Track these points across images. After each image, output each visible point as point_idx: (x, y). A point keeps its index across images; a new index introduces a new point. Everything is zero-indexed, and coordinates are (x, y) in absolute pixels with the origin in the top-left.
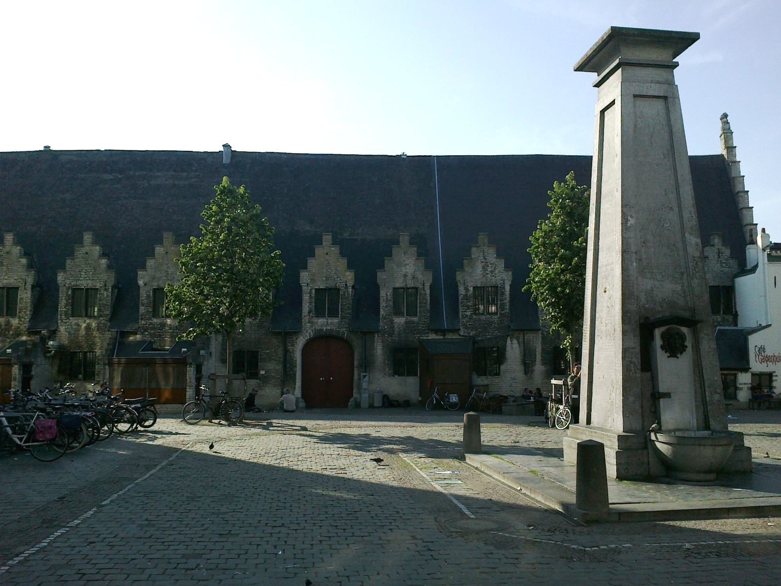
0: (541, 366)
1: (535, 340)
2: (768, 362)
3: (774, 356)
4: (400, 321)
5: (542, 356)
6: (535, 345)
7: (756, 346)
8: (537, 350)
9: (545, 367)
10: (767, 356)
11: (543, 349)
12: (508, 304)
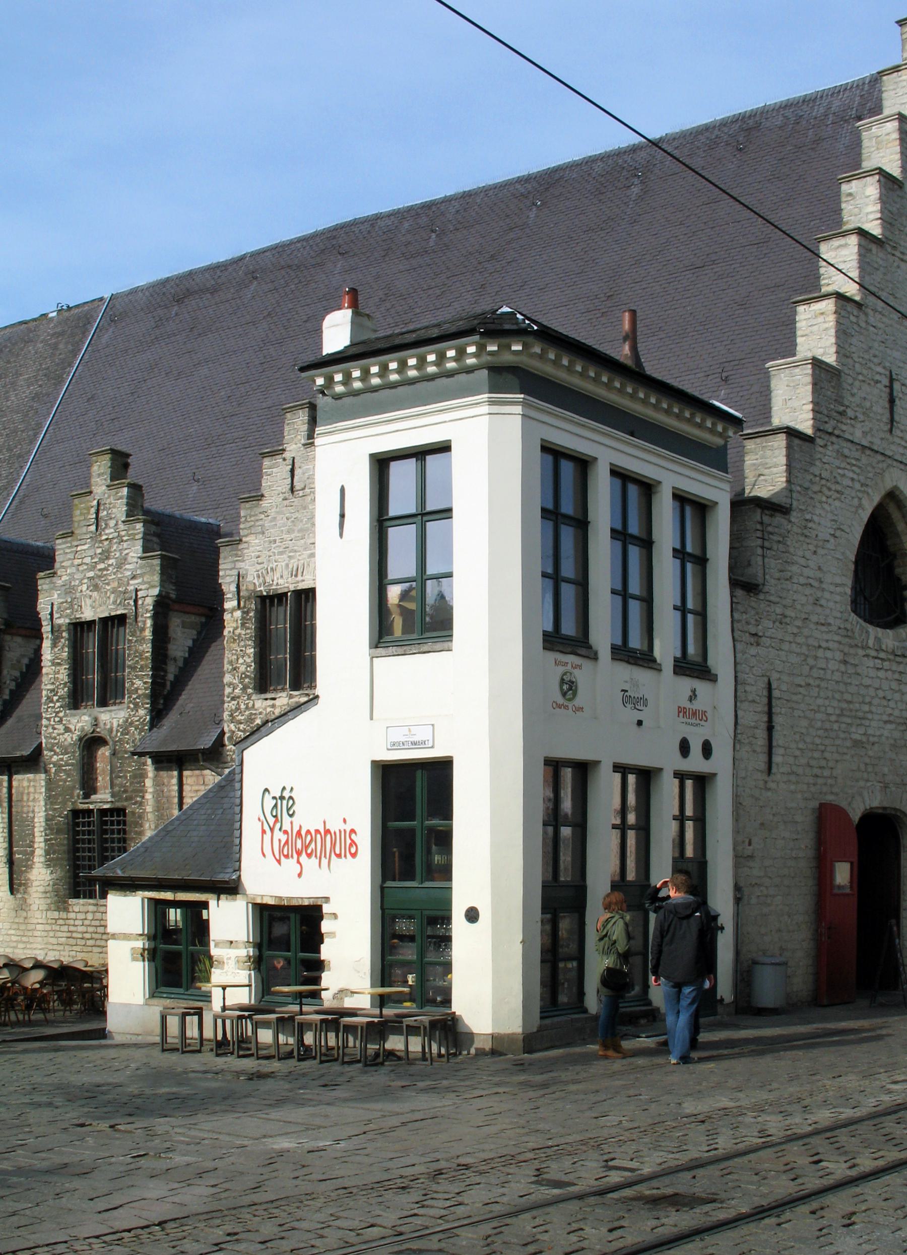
0: (44, 871)
1: (32, 790)
2: (303, 858)
3: (327, 832)
5: (46, 841)
6: (31, 804)
7: (266, 790)
8: (36, 820)
9: (52, 873)
10: (299, 833)
11: (48, 819)
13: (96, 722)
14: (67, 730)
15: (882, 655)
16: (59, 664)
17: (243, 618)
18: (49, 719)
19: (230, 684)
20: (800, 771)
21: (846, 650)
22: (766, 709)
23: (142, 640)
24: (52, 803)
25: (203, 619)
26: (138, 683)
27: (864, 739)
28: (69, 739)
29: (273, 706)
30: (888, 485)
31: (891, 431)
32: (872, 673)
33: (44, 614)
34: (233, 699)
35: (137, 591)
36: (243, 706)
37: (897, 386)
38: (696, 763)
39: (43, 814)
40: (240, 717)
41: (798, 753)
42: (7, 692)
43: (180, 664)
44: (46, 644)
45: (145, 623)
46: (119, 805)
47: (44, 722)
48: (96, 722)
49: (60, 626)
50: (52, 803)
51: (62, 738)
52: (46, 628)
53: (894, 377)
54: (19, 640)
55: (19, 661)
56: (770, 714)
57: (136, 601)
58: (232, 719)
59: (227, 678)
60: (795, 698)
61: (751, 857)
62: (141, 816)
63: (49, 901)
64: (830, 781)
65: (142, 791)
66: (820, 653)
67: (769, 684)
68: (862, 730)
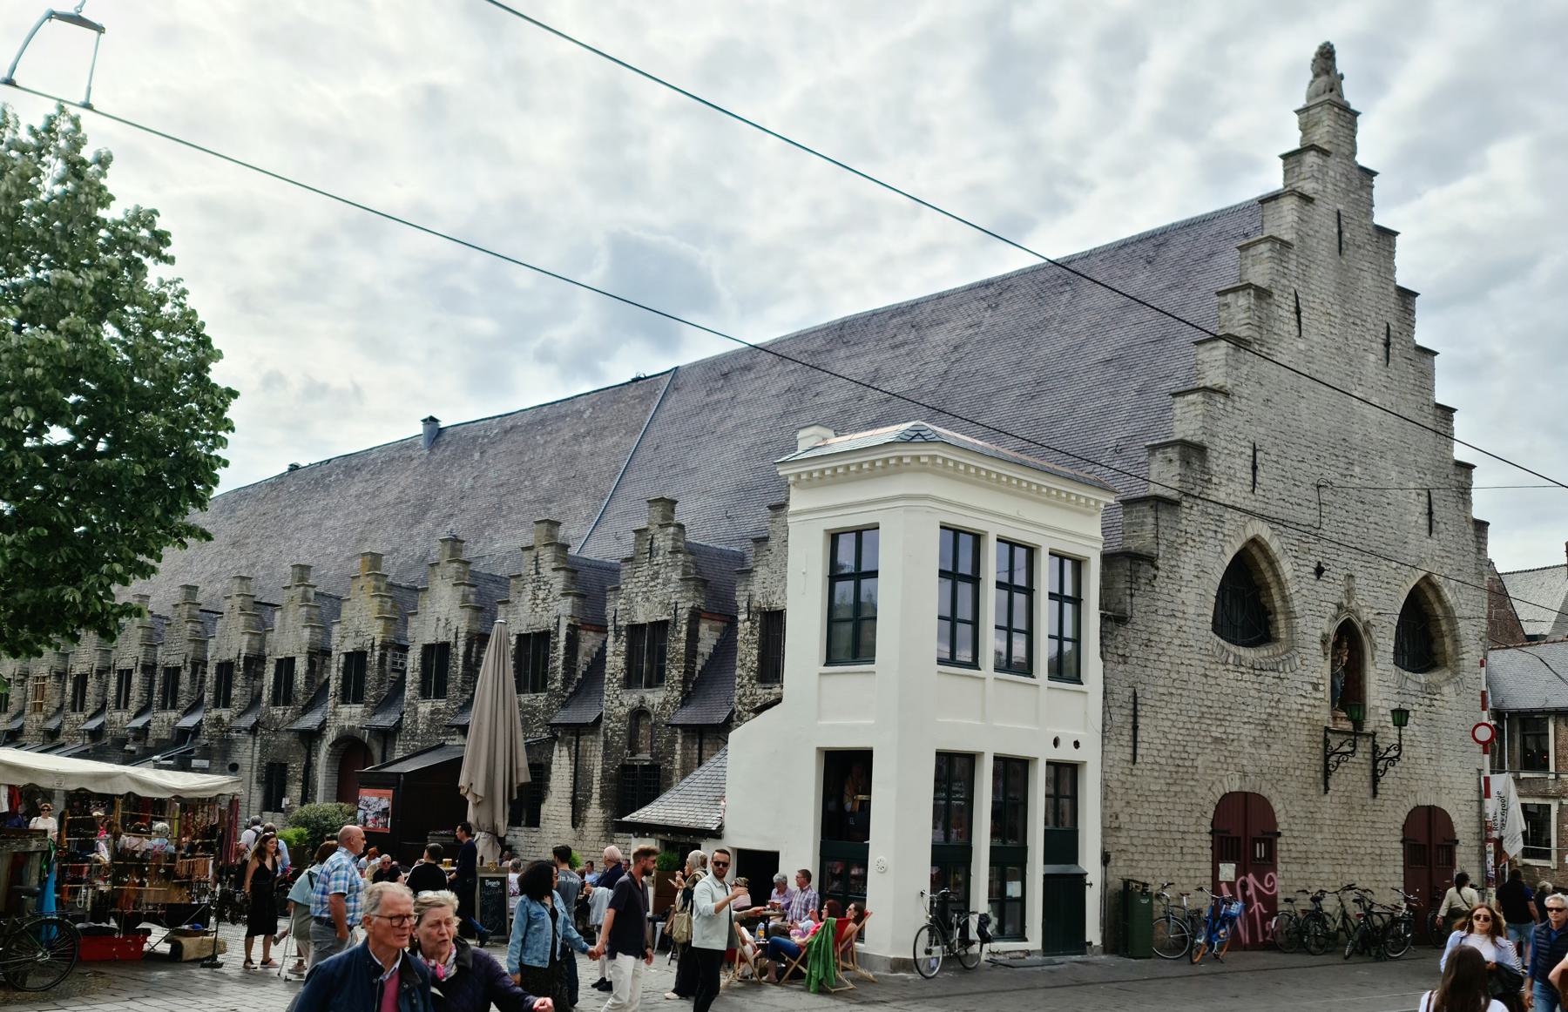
0: (598, 811)
1: (593, 748)
4: (425, 708)
5: (601, 787)
11: (603, 771)
12: (560, 669)
13: (642, 700)
14: (621, 704)
15: (1243, 669)
16: (618, 655)
17: (751, 627)
18: (609, 696)
19: (740, 676)
20: (1163, 761)
21: (1207, 666)
22: (1132, 713)
23: (679, 640)
24: (607, 759)
25: (725, 625)
26: (674, 672)
27: (1224, 736)
28: (623, 711)
29: (770, 694)
30: (1250, 534)
31: (1253, 491)
32: (1233, 683)
33: (610, 618)
34: (741, 687)
35: (676, 603)
36: (748, 693)
37: (1259, 454)
38: (1065, 754)
39: (600, 767)
40: (745, 701)
41: (1161, 747)
42: (581, 673)
43: (707, 657)
44: (611, 639)
45: (681, 627)
46: (656, 762)
47: (606, 698)
48: (642, 700)
49: (620, 627)
50: (607, 759)
51: (617, 710)
52: (611, 627)
53: (1258, 447)
54: (592, 634)
55: (590, 650)
56: (1135, 716)
57: (675, 611)
58: (740, 702)
59: (738, 671)
60: (1158, 704)
61: (1118, 828)
62: (671, 772)
63: (600, 834)
64: (1190, 770)
65: (673, 752)
66: (1183, 669)
67: (1135, 693)
68: (1222, 729)
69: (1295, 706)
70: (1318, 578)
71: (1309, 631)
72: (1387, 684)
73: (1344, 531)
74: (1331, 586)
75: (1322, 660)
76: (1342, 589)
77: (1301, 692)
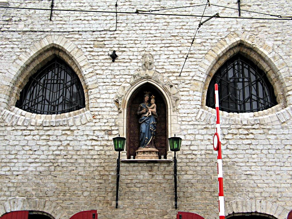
27: (8, 173)
69: (84, 147)
70: (113, 61)
71: (103, 96)
72: (191, 123)
73: (141, 28)
74: (127, 64)
75: (117, 113)
76: (140, 64)
77: (91, 137)
